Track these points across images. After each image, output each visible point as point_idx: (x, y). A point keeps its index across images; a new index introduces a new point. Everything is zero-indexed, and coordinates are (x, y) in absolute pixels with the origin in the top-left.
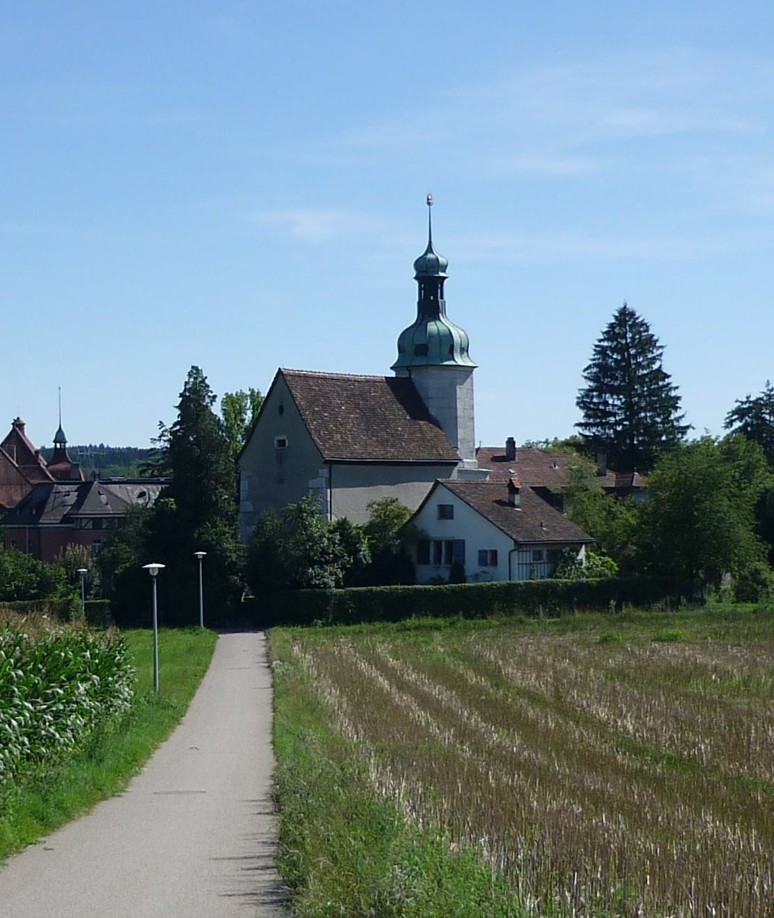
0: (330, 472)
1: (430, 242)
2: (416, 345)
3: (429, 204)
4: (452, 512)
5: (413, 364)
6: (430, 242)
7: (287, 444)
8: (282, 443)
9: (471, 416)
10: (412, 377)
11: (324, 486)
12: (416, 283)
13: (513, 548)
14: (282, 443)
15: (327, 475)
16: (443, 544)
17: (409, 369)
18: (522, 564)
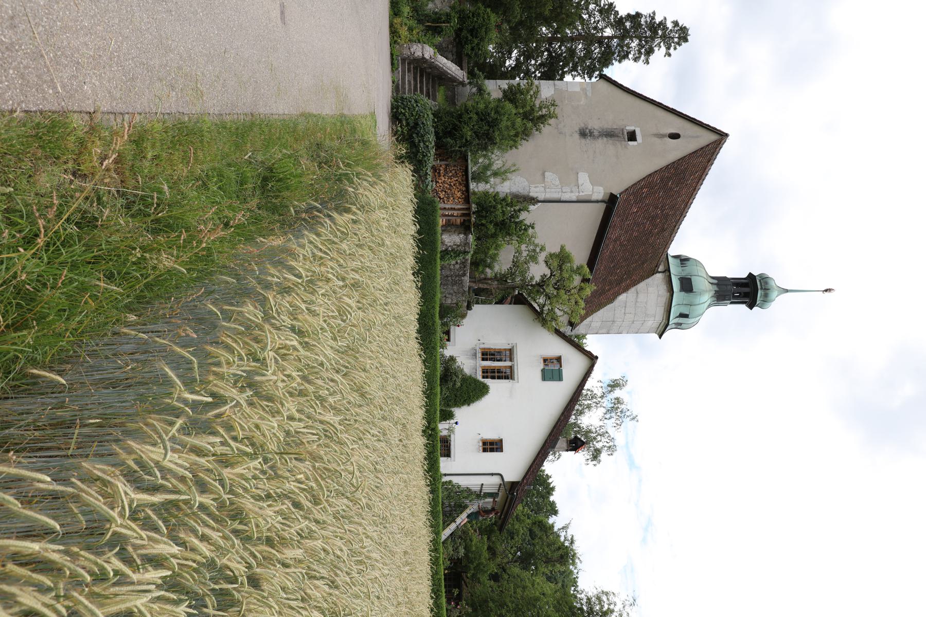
0: (597, 202)
1: (787, 291)
2: (690, 279)
3: (826, 291)
4: (552, 379)
5: (672, 276)
6: (787, 291)
7: (631, 143)
8: (632, 136)
9: (610, 332)
10: (657, 274)
11: (581, 194)
12: (744, 275)
13: (506, 479)
14: (632, 136)
15: (594, 198)
16: (508, 364)
17: (668, 270)
18: (482, 487)
